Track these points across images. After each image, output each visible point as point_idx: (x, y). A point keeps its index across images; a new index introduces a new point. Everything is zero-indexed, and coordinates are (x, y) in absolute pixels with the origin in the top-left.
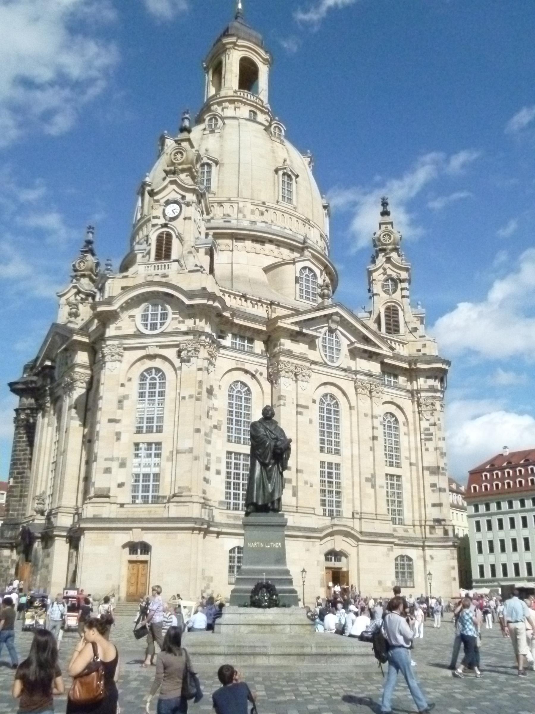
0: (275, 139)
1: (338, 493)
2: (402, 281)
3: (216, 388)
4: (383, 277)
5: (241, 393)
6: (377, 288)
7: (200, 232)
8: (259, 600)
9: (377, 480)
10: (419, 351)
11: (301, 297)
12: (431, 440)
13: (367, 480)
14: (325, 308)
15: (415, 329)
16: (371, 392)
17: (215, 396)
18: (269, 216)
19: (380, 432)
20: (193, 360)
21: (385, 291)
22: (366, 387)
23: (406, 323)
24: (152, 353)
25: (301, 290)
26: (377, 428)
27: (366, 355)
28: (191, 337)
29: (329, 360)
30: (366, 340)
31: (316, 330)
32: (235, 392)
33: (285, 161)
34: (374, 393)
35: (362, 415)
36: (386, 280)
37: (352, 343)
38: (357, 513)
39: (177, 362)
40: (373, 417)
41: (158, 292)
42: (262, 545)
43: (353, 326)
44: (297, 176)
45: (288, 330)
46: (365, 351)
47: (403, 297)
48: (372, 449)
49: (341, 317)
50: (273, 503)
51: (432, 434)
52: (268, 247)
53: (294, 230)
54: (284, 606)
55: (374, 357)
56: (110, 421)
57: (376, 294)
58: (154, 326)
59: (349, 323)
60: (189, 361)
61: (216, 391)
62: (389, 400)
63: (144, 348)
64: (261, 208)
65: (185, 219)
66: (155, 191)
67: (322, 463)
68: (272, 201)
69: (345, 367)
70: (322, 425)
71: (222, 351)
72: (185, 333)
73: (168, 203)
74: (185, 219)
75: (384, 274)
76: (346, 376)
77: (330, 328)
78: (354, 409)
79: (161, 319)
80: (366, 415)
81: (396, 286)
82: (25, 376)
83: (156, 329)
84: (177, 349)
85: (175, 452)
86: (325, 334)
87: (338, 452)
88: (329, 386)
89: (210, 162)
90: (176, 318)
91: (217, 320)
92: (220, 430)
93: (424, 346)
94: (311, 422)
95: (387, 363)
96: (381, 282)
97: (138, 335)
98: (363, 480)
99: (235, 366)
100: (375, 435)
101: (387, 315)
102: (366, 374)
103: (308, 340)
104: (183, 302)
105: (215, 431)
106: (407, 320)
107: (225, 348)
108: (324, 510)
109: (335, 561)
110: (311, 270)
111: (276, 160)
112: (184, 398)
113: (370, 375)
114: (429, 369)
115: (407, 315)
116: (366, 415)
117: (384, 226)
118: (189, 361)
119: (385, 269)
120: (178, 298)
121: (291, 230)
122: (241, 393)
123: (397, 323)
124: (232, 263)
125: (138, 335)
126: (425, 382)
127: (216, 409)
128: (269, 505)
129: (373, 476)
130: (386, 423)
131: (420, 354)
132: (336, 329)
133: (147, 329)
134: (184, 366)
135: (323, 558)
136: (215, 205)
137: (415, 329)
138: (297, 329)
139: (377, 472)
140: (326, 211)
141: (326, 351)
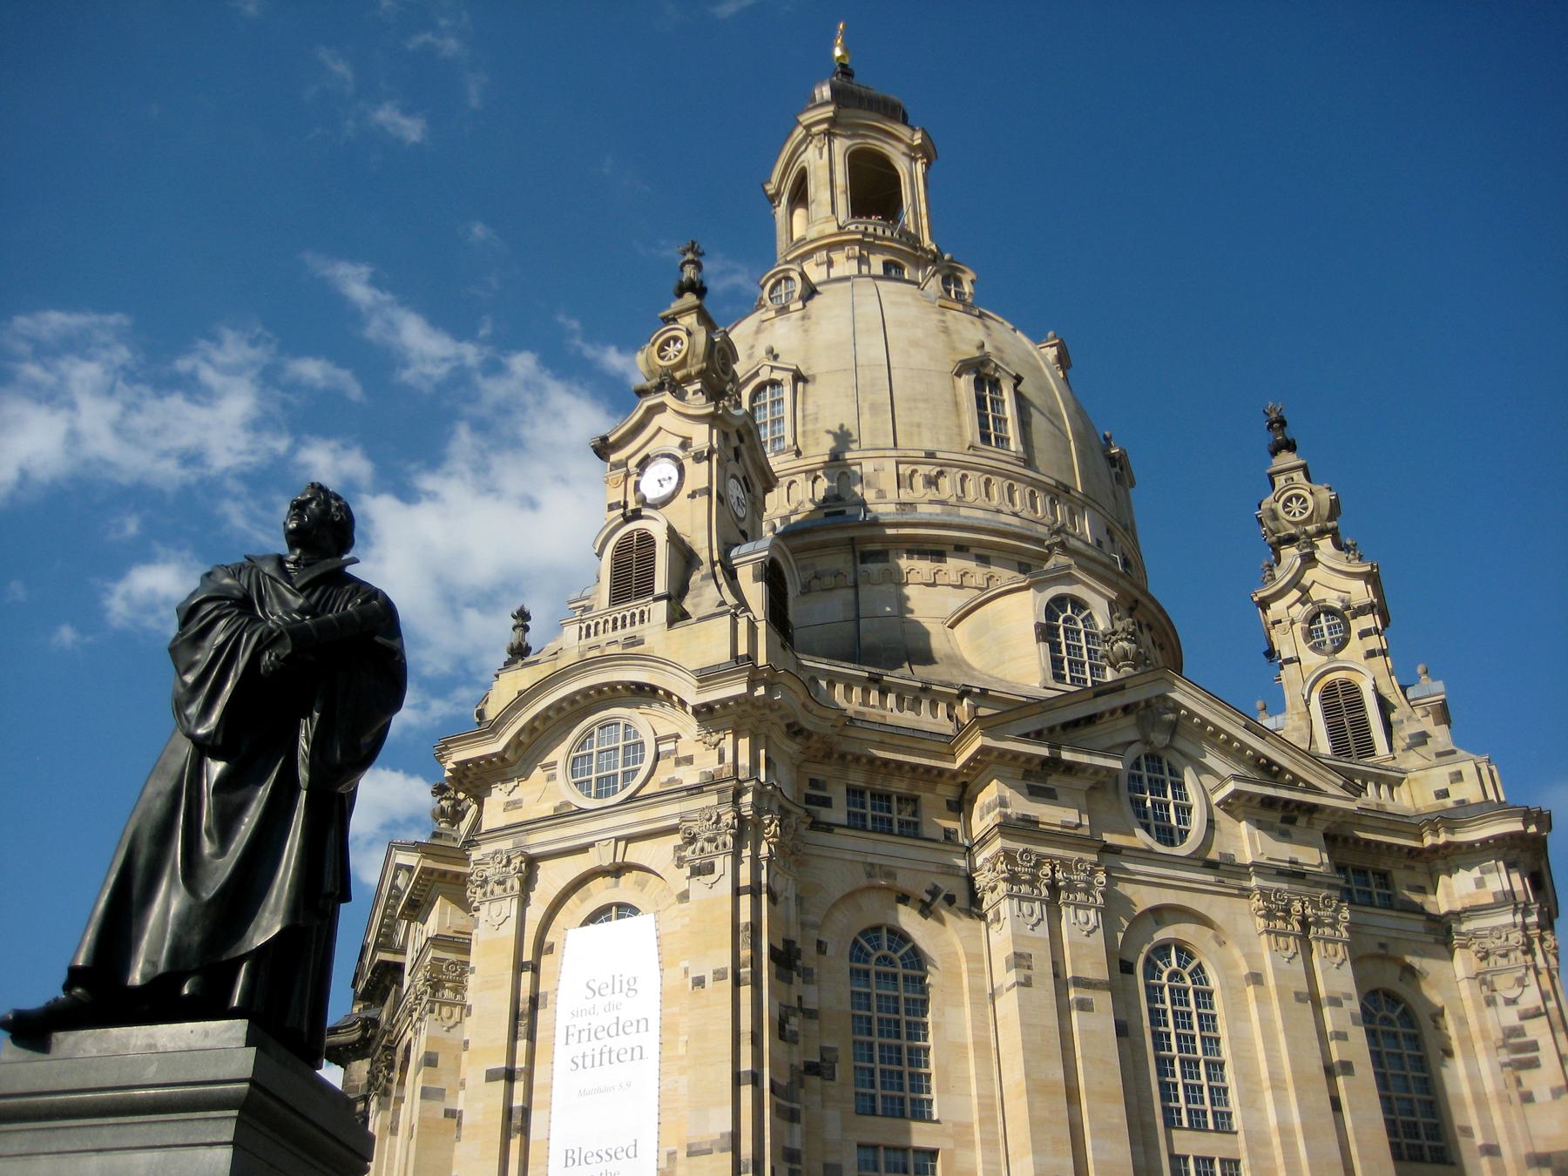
0: (949, 304)
2: (1361, 611)
3: (810, 950)
4: (1299, 611)
5: (892, 963)
6: (1288, 642)
7: (744, 534)
10: (1444, 794)
11: (1059, 677)
12: (1533, 1064)
14: (1122, 688)
15: (1422, 738)
17: (807, 975)
18: (947, 486)
19: (1356, 1047)
20: (718, 862)
21: (1314, 648)
24: (607, 861)
25: (1056, 663)
26: (1341, 1036)
27: (1275, 816)
28: (712, 799)
29: (1159, 840)
30: (1268, 770)
31: (1106, 752)
32: (874, 959)
33: (982, 346)
36: (1314, 619)
39: (679, 878)
41: (612, 686)
44: (1018, 379)
45: (1016, 756)
46: (1269, 802)
47: (1371, 654)
48: (1336, 1105)
51: (1534, 1046)
52: (953, 565)
53: (1024, 514)
55: (1302, 821)
56: (491, 1076)
57: (1290, 661)
58: (605, 786)
60: (710, 869)
61: (809, 957)
63: (584, 849)
64: (923, 470)
65: (692, 496)
66: (611, 439)
68: (957, 449)
70: (1160, 1040)
71: (821, 837)
72: (696, 790)
73: (643, 464)
74: (692, 496)
75: (1304, 604)
76: (1220, 883)
77: (1147, 742)
79: (626, 763)
81: (1348, 630)
82: (356, 1010)
83: (615, 792)
84: (677, 839)
85: (682, 1155)
86: (1137, 765)
87: (1223, 1123)
89: (777, 375)
90: (669, 753)
91: (792, 747)
92: (832, 1078)
93: (1457, 777)
94: (1122, 1030)
96: (1298, 627)
97: (563, 815)
99: (864, 882)
101: (1330, 711)
102: (1281, 873)
103: (1081, 784)
104: (683, 703)
105: (815, 1081)
107: (829, 828)
110: (1079, 605)
111: (954, 349)
112: (699, 982)
113: (1295, 874)
114: (1484, 842)
117: (1283, 478)
118: (710, 869)
119: (1305, 591)
120: (669, 694)
121: (1015, 514)
122: (892, 963)
123: (1362, 726)
124: (858, 618)
125: (563, 815)
126: (1480, 883)
127: (811, 1014)
131: (1448, 803)
132: (1169, 747)
133: (589, 795)
134: (698, 887)
136: (800, 478)
138: (1044, 751)
140: (1117, 469)
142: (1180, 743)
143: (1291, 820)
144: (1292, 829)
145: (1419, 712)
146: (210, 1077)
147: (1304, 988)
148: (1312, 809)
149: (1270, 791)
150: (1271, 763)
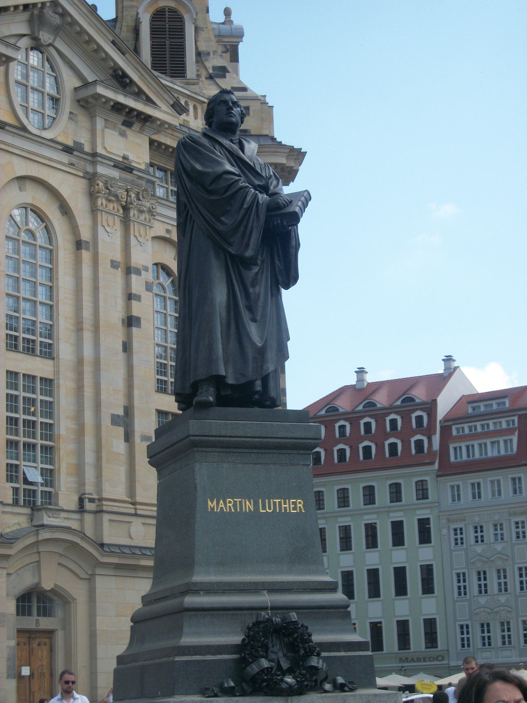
1: (48, 450)
8: (268, 670)
9: (137, 421)
13: (115, 420)
16: (126, 209)
22: (116, 196)
23: (198, 54)
26: (138, 298)
27: (118, 119)
30: (121, 80)
34: (133, 213)
35: (104, 266)
37: (86, 84)
38: (92, 500)
40: (129, 271)
42: (249, 506)
43: (91, 40)
46: (118, 108)
48: (127, 347)
49: (64, 14)
50: (265, 380)
54: (341, 688)
59: (82, 31)
62: (163, 234)
67: (12, 375)
69: (70, 143)
76: (72, 164)
77: (35, 39)
78: (87, 249)
80: (114, 265)
88: (29, 186)
95: (160, 144)
98: (106, 421)
100: (135, 313)
102: (117, 166)
106: (203, 47)
108: (16, 491)
109: (39, 615)
113: (125, 166)
115: (203, 35)
116: (114, 265)
128: (258, 386)
129: (128, 410)
130: (156, 289)
132: (50, 45)
135: (11, 607)
137: (222, 72)
139: (137, 403)
141: (26, 99)
142: (60, 44)
143: (128, 124)
144: (129, 132)
145: (220, 49)
146: (303, 436)
147: (118, 257)
148: (146, 119)
149: (121, 99)
150: (125, 75)
